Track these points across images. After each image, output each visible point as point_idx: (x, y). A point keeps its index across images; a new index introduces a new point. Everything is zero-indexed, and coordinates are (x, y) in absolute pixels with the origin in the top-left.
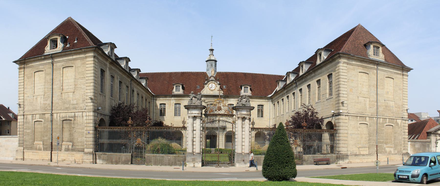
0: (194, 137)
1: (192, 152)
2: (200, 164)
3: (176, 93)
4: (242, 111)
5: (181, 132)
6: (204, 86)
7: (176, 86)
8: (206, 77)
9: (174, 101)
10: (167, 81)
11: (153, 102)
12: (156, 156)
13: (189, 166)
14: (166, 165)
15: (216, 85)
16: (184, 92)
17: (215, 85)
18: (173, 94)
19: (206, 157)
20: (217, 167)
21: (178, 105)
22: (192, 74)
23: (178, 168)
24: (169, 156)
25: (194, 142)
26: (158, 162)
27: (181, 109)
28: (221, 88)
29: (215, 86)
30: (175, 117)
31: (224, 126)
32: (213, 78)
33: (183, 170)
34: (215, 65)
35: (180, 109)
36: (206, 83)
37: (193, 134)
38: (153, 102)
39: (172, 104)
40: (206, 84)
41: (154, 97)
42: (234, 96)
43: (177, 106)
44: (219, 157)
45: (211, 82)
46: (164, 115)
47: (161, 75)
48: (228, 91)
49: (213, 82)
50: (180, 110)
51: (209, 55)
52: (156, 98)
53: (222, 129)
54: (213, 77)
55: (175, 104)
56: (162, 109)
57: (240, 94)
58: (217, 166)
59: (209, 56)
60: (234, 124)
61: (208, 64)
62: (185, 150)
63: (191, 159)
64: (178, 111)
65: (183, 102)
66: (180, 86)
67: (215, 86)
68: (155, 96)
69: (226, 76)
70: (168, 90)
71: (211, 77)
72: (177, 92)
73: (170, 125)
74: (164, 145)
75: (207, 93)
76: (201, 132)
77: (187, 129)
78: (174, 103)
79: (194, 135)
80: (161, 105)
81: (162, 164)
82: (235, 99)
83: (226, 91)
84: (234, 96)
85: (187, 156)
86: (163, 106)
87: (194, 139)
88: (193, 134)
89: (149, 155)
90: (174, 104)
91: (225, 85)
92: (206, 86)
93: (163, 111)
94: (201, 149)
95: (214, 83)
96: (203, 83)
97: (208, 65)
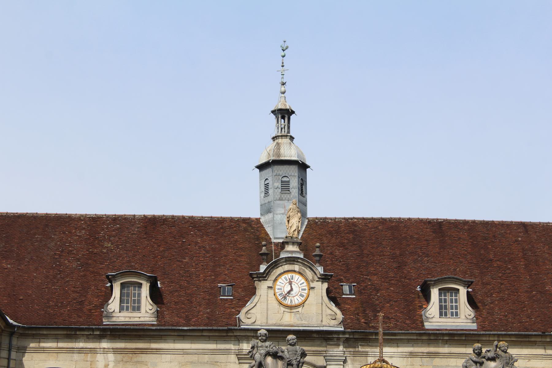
3: (122, 319)
6: (255, 288)
7: (121, 284)
8: (264, 243)
10: (78, 260)
11: (9, 359)
15: (309, 284)
16: (159, 315)
17: (307, 280)
18: (105, 322)
22: (194, 227)
28: (330, 295)
29: (306, 288)
32: (295, 248)
34: (302, 185)
38: (6, 361)
40: (264, 277)
41: (12, 334)
42: (395, 334)
45: (287, 267)
47: (47, 226)
48: (365, 311)
49: (296, 267)
51: (274, 138)
52: (22, 343)
54: (293, 243)
57: (422, 322)
59: (272, 145)
61: (270, 181)
66: (140, 285)
68: (21, 332)
69: (351, 236)
70: (81, 303)
71: (282, 246)
72: (125, 314)
75: (270, 322)
82: (400, 349)
83: (356, 308)
84: (395, 334)
91: (347, 281)
92: (262, 287)
95: (300, 273)
96: (251, 275)
97: (267, 186)
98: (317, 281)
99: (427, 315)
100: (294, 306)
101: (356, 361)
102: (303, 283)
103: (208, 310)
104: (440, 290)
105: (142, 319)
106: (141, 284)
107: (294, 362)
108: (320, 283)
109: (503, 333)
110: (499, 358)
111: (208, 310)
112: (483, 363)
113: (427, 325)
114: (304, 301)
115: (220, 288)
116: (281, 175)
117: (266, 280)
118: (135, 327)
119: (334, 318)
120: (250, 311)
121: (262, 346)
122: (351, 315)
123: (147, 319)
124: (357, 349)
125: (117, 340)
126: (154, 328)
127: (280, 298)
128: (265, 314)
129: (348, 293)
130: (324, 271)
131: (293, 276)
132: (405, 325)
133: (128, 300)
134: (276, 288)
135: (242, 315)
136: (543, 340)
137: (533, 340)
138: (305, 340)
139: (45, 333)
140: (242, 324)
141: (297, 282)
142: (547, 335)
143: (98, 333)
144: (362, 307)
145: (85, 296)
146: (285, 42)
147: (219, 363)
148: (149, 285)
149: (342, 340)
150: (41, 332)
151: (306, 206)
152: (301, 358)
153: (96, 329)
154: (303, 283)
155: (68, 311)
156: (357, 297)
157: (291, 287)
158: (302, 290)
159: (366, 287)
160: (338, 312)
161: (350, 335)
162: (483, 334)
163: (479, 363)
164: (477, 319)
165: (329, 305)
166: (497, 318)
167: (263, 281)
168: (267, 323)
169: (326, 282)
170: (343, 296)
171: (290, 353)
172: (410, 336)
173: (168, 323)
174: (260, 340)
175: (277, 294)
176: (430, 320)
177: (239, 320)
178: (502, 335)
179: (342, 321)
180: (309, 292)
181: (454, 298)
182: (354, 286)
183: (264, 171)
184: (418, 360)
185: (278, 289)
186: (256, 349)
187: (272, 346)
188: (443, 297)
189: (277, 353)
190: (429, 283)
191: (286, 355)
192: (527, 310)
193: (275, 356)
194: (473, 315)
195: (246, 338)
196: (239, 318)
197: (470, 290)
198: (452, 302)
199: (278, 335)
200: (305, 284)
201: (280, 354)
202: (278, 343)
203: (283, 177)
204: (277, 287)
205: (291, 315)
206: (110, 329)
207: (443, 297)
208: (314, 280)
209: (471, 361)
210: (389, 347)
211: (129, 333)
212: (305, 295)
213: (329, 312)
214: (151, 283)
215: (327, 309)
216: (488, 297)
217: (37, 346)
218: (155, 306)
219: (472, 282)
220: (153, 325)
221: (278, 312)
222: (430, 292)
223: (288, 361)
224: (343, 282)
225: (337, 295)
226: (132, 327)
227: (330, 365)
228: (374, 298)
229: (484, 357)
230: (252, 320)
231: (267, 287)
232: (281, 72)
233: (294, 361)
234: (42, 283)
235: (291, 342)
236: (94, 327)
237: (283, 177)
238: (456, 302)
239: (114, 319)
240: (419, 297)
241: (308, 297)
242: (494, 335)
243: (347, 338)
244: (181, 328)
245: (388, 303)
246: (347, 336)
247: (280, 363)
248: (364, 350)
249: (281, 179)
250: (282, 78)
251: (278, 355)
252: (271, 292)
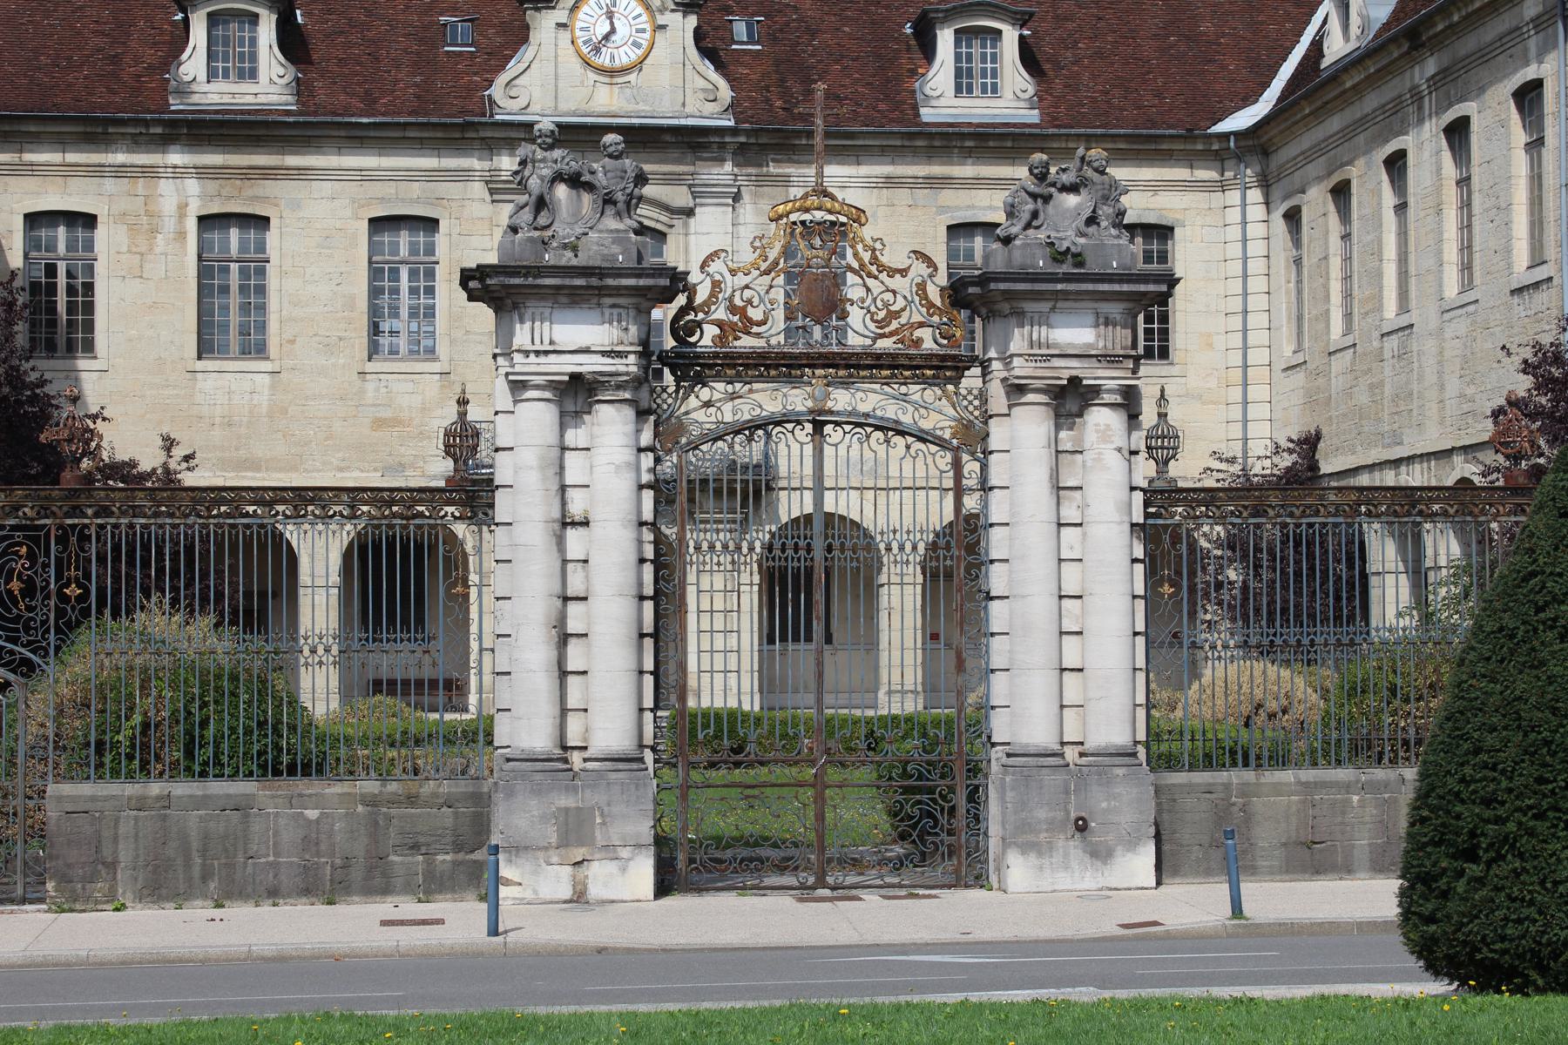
0: (569, 594)
1: (558, 751)
2: (643, 871)
3: (215, 99)
4: (1055, 318)
5: (279, 537)
6: (527, 28)
7: (209, 15)
9: (192, 186)
12: (166, 800)
13: (529, 895)
14: (274, 894)
15: (653, 17)
16: (301, 88)
18: (175, 104)
19: (692, 793)
20: (805, 892)
21: (234, 234)
23: (424, 922)
24: (304, 800)
25: (574, 648)
26: (188, 865)
27: (273, 282)
28: (702, 44)
29: (647, 26)
30: (200, 365)
31: (745, 468)
33: (494, 931)
35: (261, 272)
37: (558, 564)
39: (169, 225)
42: (851, 136)
43: (395, 249)
44: (820, 800)
46: (71, 348)
48: (783, 80)
50: (261, 290)
53: (732, 492)
55: (203, 220)
56: (51, 270)
57: (915, 108)
58: (803, 887)
60: (973, 454)
62: (481, 733)
63: (544, 818)
64: (235, 300)
65: (296, 205)
66: (254, 19)
67: (644, 21)
70: (115, 60)
72: (220, 86)
73: (149, 459)
74: (204, 684)
75: (563, 107)
76: (640, 542)
77: (501, 514)
78: (195, 209)
79: (570, 566)
80: (43, 233)
81: (233, 890)
82: (864, 170)
84: (851, 136)
85: (510, 794)
86: (61, 248)
87: (574, 609)
88: (565, 562)
89: (86, 789)
90: (192, 225)
91: (744, 11)
93: (62, 299)
94: (641, 710)
98: (673, 11)
99: (928, 91)
102: (640, 15)
103: (418, 79)
104: (956, 31)
105: (262, 99)
106: (257, 16)
107: (620, 197)
108: (679, 15)
109: (1099, 131)
110: (1086, 186)
111: (418, 79)
112: (1051, 196)
113: (927, 115)
115: (445, 25)
117: (554, 8)
118: (247, 117)
119: (712, 98)
120: (517, 82)
121: (543, 160)
122: (750, 91)
123: (274, 99)
124: (765, 169)
125: (205, 148)
126: (291, 119)
127: (585, 50)
128: (552, 87)
129: (745, 39)
132: (876, 115)
133: (226, 54)
135: (497, 91)
136: (1189, 147)
137: (1164, 147)
139: (33, 129)
140: (498, 111)
141: (625, 13)
142: (1196, 137)
143: (159, 130)
144: (777, 72)
145: (124, 43)
148: (274, 17)
149: (731, 148)
150: (24, 128)
152: (636, 186)
153: (153, 120)
154: (640, 15)
155: (86, 78)
157: (612, 24)
158: (638, 31)
159: (787, 24)
160: (722, 83)
161: (748, 137)
162: (1053, 135)
163: (1041, 196)
164: (1040, 99)
165: (701, 68)
166: (1086, 97)
168: (556, 108)
169: (692, 12)
170: (734, 47)
171: (609, 175)
172: (888, 138)
173: (325, 107)
174: (540, 145)
175: (580, 42)
176: (934, 103)
177: (492, 101)
178: (1095, 136)
179: (731, 106)
181: (989, 51)
182: (758, 22)
184: (903, 195)
185: (582, 29)
186: (530, 166)
187: (567, 160)
188: (964, 50)
189: (579, 174)
190: (932, 15)
191: (601, 179)
192: (1155, 79)
193: (575, 181)
194: (1031, 90)
196: (490, 96)
197: (1026, 32)
198: (984, 61)
199: (582, 138)
200: (644, 18)
201: (586, 178)
204: (579, 24)
206: (187, 121)
207: (964, 50)
208: (666, 9)
209: (1024, 194)
210: (838, 164)
211: (232, 132)
212: (645, 44)
213: (701, 83)
214: (279, 14)
215: (697, 77)
216: (1067, 48)
217: (17, 160)
218: (292, 68)
219: (1031, 15)
220: (288, 113)
222: (935, 36)
223: (606, 194)
224: (731, 13)
225: (719, 44)
226: (239, 117)
227: (702, 205)
228: (804, 52)
229: (1053, 185)
230: (522, 102)
233: (620, 193)
234: (18, 12)
235: (611, 149)
236: (148, 116)
238: (994, 60)
239: (195, 99)
240: (908, 50)
242: (1079, 136)
243: (742, 143)
244: (353, 120)
245: (837, 62)
246: (742, 139)
247: (587, 198)
248: (780, 171)
251: (583, 179)
252: (565, 36)
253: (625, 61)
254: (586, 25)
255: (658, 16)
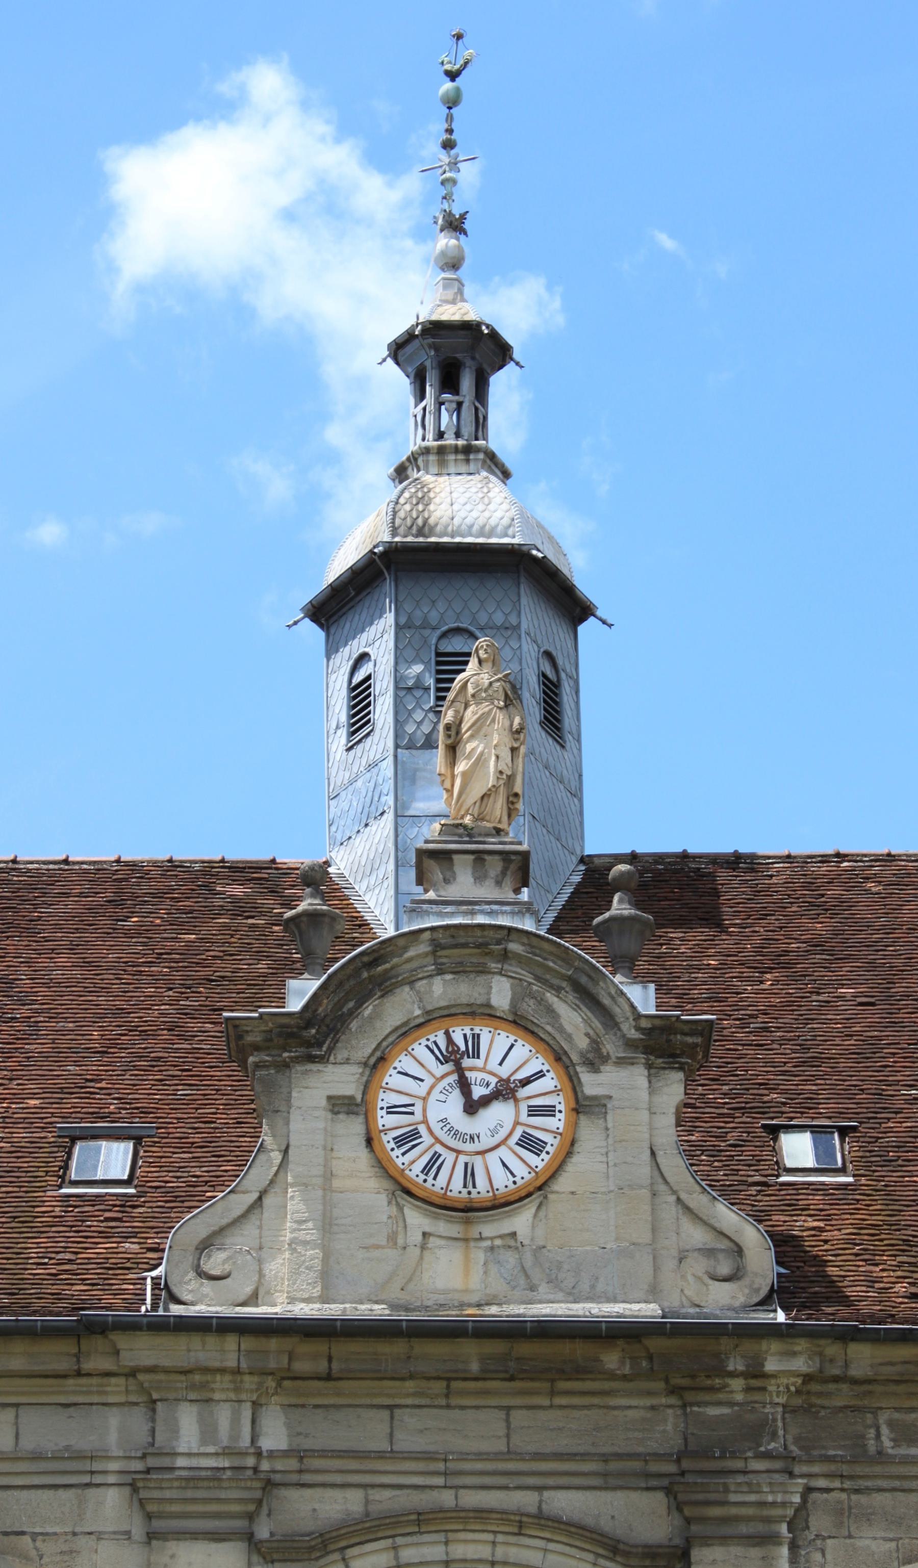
15: (573, 1082)
17: (559, 1057)
29: (559, 1102)
36: (295, 1005)
98: (621, 1062)
100: (489, 1204)
101: (867, 1517)
108: (638, 1076)
114: (548, 1174)
116: (434, 623)
117: (322, 1059)
130: (658, 1006)
131: (476, 1038)
134: (380, 1104)
138: (553, 1393)
146: (459, 37)
147: (27, 1539)
151: (577, 794)
154: (540, 1075)
156: (863, 1181)
167: (299, 1068)
175: (388, 1140)
180: (573, 1126)
183: (348, 625)
185: (392, 1110)
195: (193, 1387)
202: (392, 1418)
203: (444, 635)
204: (388, 1098)
205: (467, 1259)
208: (605, 1059)
213: (697, 1236)
221: (392, 1239)
231: (324, 1102)
232: (441, 171)
237: (444, 635)
241: (569, 1154)
249: (434, 641)
250: (444, 198)
252: (355, 1127)
253: (502, 1181)
254: (406, 1100)
255: (586, 1077)
